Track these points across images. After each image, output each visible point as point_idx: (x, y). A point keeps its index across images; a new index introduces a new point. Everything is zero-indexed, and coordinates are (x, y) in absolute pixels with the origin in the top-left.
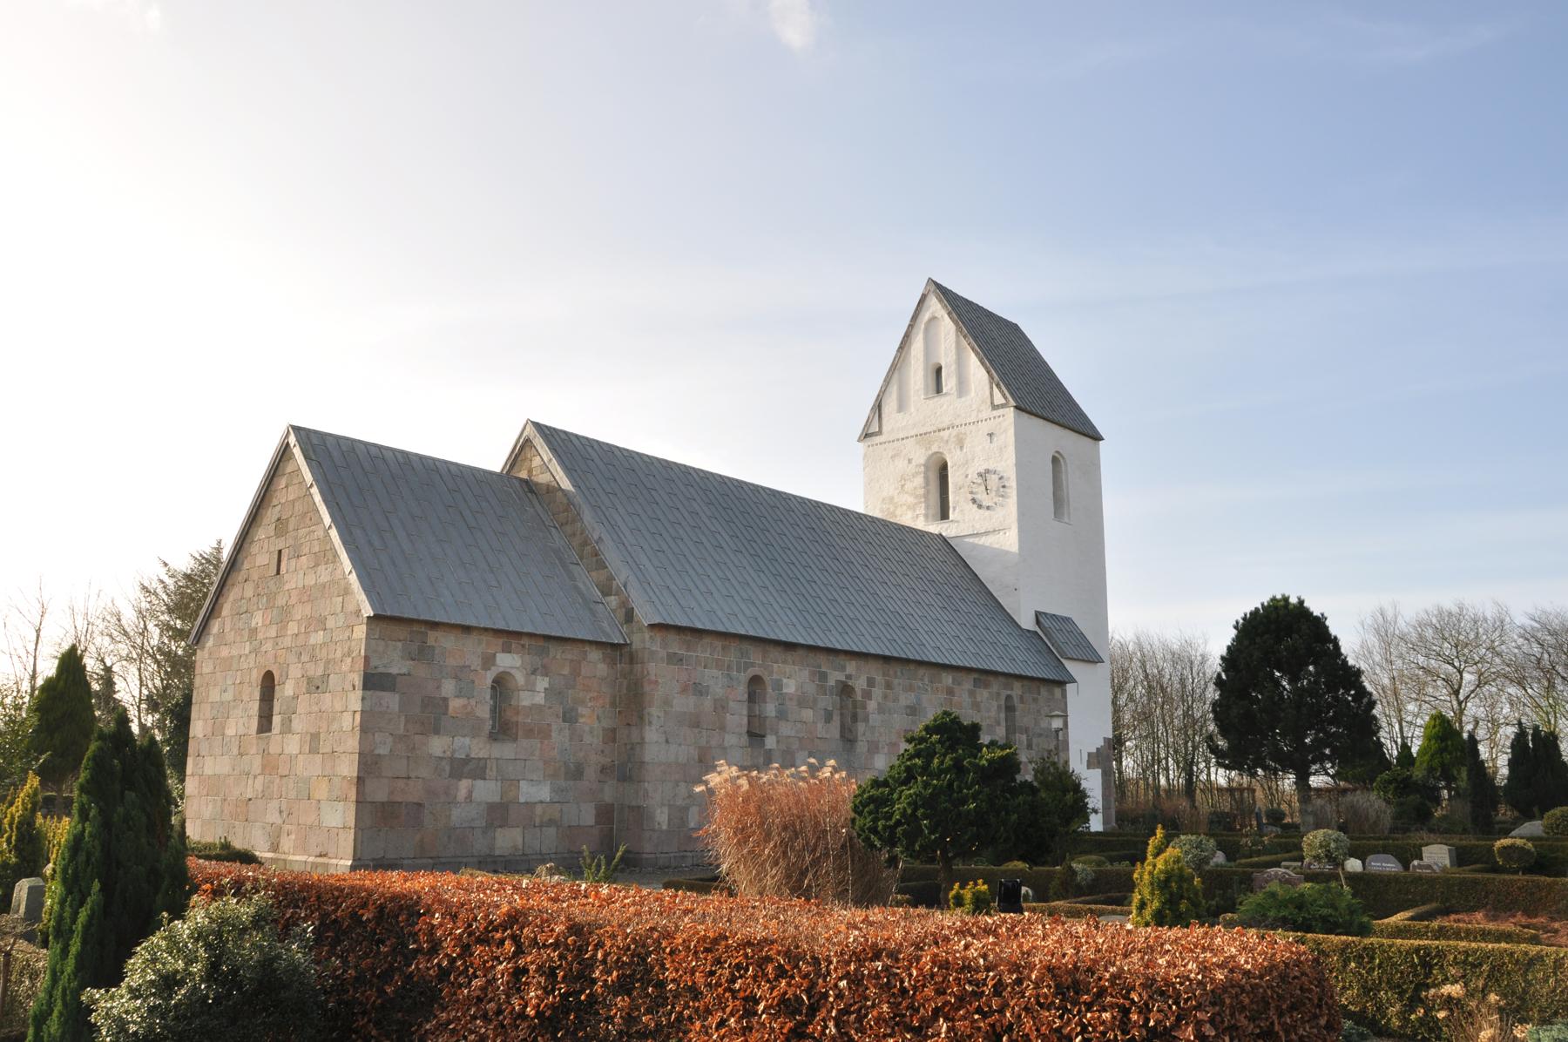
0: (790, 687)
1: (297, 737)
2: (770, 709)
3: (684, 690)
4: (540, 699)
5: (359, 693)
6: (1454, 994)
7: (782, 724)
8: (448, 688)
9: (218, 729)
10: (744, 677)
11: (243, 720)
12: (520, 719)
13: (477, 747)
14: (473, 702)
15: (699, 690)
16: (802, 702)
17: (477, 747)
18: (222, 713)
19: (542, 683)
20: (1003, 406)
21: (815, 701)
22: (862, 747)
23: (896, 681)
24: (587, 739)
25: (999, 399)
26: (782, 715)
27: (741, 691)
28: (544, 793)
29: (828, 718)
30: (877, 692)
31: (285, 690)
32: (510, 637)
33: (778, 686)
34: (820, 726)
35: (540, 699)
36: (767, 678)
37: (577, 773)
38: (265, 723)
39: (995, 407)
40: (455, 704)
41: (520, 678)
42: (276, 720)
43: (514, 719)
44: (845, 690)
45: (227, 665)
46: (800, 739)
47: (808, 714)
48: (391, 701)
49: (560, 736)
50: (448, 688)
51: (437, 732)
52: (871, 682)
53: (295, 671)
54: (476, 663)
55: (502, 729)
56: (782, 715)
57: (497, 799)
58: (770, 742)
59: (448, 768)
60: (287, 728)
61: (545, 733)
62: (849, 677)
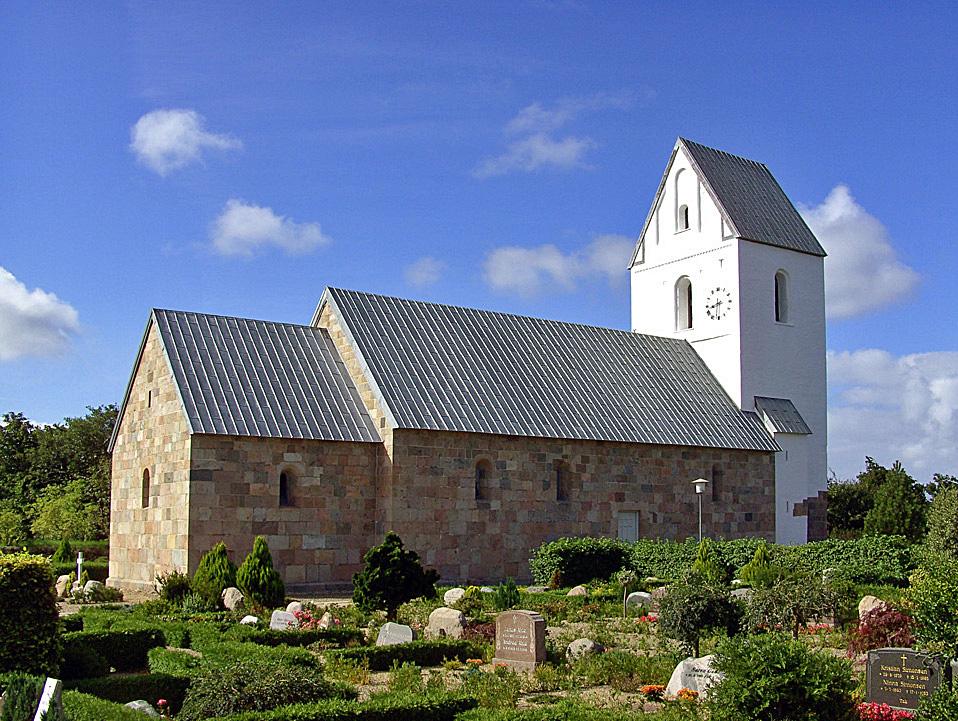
0: (512, 466)
1: (161, 511)
2: (494, 482)
3: (423, 472)
4: (317, 482)
5: (188, 482)
6: (277, 613)
7: (506, 493)
8: (249, 477)
9: (123, 506)
10: (474, 461)
11: (136, 502)
12: (302, 495)
13: (273, 514)
14: (267, 485)
15: (435, 471)
16: (523, 476)
17: (273, 514)
18: (125, 493)
19: (318, 471)
20: (730, 237)
21: (535, 476)
22: (576, 506)
23: (608, 458)
24: (353, 507)
25: (728, 232)
26: (505, 486)
27: (472, 471)
28: (321, 543)
29: (547, 486)
30: (591, 467)
31: (154, 481)
32: (293, 444)
33: (503, 465)
34: (538, 492)
35: (317, 482)
36: (492, 460)
37: (346, 528)
38: (145, 504)
39: (724, 239)
40: (254, 488)
41: (301, 469)
42: (151, 499)
43: (298, 496)
44: (560, 468)
45: (127, 465)
46: (522, 503)
47: (527, 485)
48: (210, 486)
49: (332, 506)
50: (249, 477)
51: (242, 505)
52: (585, 460)
53: (158, 470)
54: (268, 459)
55: (286, 498)
56: (505, 486)
57: (286, 547)
58: (495, 505)
59: (251, 528)
60: (156, 506)
61: (321, 504)
62: (566, 457)
